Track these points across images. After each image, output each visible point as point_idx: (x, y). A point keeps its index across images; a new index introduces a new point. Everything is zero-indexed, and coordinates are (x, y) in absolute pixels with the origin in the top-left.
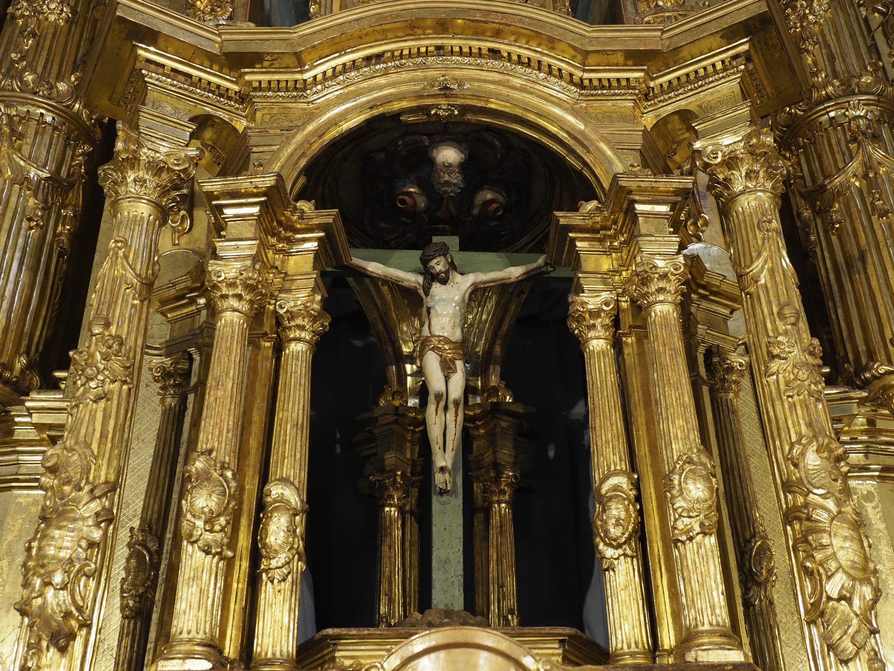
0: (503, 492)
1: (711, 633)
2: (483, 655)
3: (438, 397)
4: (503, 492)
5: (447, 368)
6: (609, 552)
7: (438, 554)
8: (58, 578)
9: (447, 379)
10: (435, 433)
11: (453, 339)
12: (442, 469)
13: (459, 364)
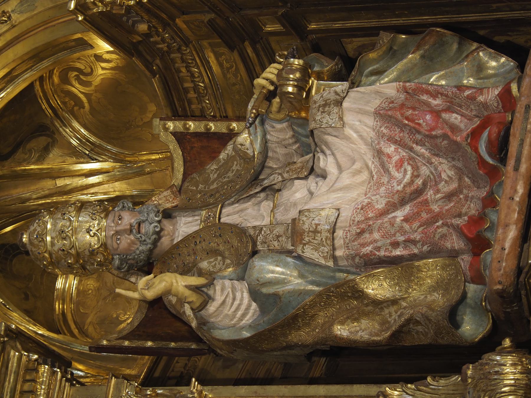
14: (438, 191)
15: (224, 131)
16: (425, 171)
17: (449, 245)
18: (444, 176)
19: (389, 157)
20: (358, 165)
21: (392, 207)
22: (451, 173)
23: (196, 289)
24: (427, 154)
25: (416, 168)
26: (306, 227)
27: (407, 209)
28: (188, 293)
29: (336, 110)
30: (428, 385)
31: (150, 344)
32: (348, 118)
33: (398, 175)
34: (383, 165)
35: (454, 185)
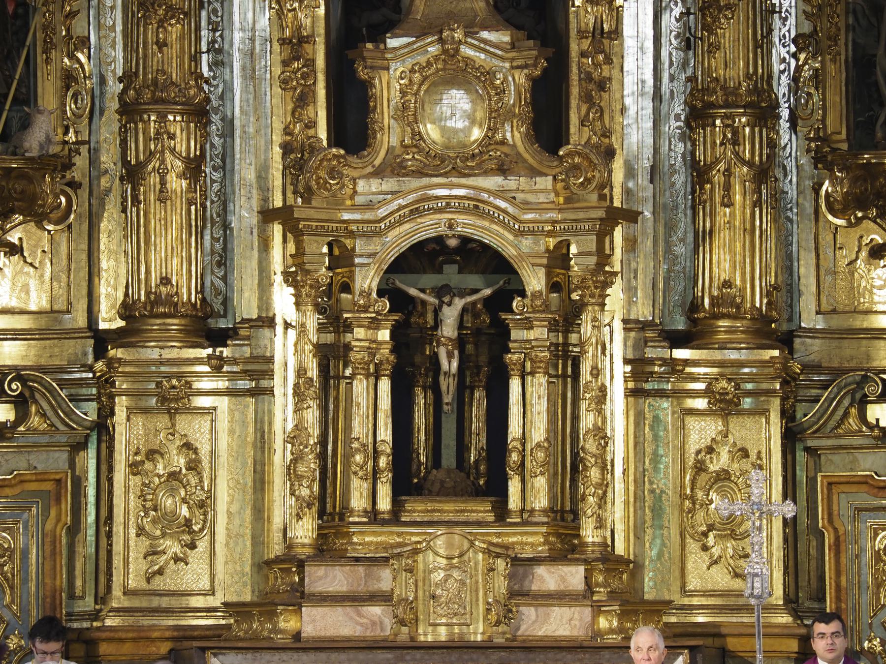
0: (480, 381)
1: (539, 511)
2: (456, 536)
3: (445, 373)
4: (480, 381)
5: (450, 356)
6: (510, 472)
7: (444, 442)
8: (304, 483)
9: (450, 362)
10: (444, 388)
11: (453, 338)
12: (447, 404)
13: (456, 353)
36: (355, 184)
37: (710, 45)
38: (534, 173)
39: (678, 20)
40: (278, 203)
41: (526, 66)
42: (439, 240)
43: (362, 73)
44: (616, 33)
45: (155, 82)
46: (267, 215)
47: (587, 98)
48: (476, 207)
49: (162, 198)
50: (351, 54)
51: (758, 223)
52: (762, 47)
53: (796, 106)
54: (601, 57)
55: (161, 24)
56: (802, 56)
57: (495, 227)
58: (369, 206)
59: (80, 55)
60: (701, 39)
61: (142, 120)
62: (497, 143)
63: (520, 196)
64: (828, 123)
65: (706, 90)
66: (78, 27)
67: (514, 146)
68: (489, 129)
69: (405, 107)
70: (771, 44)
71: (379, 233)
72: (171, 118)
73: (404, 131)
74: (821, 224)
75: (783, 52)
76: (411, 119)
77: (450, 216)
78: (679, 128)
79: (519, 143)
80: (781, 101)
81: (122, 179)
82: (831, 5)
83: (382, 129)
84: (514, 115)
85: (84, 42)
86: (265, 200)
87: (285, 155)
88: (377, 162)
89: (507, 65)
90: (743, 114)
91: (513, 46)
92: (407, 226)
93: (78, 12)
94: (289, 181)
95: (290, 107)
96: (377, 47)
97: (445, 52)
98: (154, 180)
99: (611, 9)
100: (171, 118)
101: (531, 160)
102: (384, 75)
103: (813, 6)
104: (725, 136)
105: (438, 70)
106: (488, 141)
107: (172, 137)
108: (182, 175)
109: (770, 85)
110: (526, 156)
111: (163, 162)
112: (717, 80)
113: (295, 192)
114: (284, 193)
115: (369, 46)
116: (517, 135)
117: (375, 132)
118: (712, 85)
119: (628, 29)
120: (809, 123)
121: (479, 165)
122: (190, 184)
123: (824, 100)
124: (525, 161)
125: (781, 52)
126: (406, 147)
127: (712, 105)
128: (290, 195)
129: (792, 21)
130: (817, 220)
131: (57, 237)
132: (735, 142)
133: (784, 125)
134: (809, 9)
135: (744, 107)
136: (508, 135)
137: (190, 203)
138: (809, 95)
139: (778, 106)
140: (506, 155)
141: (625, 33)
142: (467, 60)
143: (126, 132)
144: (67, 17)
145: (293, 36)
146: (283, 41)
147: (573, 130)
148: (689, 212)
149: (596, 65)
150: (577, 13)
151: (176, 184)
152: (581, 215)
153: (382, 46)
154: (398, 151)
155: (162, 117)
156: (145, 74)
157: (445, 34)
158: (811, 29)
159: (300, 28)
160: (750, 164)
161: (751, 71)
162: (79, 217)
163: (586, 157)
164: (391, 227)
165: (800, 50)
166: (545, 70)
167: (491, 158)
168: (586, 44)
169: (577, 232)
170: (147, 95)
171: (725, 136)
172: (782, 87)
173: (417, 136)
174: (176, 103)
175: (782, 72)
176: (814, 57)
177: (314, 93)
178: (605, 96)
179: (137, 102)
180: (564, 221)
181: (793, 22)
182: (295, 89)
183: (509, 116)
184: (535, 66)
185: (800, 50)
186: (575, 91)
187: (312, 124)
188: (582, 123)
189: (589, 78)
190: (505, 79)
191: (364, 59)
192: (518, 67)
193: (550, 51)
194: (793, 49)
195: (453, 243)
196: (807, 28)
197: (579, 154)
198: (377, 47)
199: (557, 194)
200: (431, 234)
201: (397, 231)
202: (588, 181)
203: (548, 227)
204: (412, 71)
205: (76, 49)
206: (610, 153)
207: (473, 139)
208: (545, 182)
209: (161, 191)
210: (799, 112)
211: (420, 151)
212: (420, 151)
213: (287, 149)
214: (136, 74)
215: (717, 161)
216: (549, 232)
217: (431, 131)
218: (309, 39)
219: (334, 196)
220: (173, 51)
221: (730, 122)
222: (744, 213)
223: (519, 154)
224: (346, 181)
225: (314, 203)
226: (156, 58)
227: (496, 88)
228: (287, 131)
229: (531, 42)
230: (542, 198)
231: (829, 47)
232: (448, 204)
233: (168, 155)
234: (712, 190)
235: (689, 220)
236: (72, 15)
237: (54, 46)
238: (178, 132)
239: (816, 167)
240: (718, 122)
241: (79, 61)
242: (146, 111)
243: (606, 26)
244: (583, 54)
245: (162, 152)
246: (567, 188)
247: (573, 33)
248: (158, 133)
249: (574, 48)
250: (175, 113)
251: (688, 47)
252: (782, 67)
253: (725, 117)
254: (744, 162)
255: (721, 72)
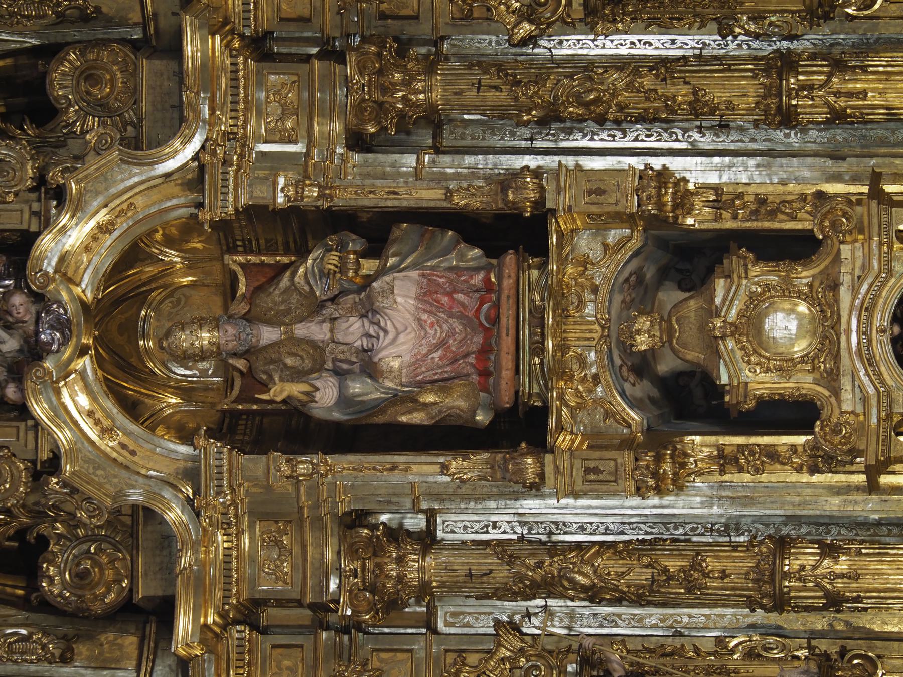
14: (455, 340)
15: (273, 262)
16: (445, 327)
17: (465, 372)
18: (457, 330)
19: (425, 322)
20: (409, 330)
21: (430, 352)
22: (460, 327)
23: (306, 393)
24: (446, 317)
25: (441, 327)
26: (384, 368)
27: (440, 352)
28: (300, 395)
29: (391, 296)
30: (470, 459)
31: (255, 407)
32: (399, 300)
33: (432, 332)
34: (421, 326)
35: (463, 335)
36: (846, 412)
37: (727, 109)
38: (837, 259)
39: (704, 136)
40: (861, 479)
41: (746, 266)
42: (894, 341)
43: (751, 405)
44: (717, 189)
45: (755, 581)
46: (872, 487)
47: (772, 214)
48: (867, 310)
49: (854, 576)
50: (734, 414)
51: (881, 69)
52: (730, 65)
53: (780, 35)
54: (738, 202)
55: (706, 575)
56: (737, 30)
57: (884, 294)
58: (865, 400)
59: (732, 645)
60: (722, 116)
61: (788, 593)
62: (811, 291)
63: (857, 272)
64: (795, 8)
65: (766, 113)
66: (708, 646)
67: (813, 276)
68: (799, 298)
69: (780, 369)
70: (725, 57)
71: (889, 394)
72: (786, 568)
73: (800, 371)
74: (881, 14)
75: (733, 46)
76: (790, 364)
77: (874, 332)
78: (796, 135)
79: (811, 272)
80: (775, 47)
81: (838, 611)
82: (694, 6)
83: (798, 389)
84: (787, 276)
85: (719, 641)
86: (858, 489)
87: (820, 472)
88: (827, 393)
89: (744, 282)
90: (787, 81)
91: (728, 277)
92: (883, 369)
93: (694, 645)
94: (842, 469)
95: (778, 467)
96: (729, 392)
97: (733, 335)
98: (839, 584)
99: (697, 193)
100: (786, 568)
101: (826, 263)
102: (751, 386)
103: (695, 21)
104: (805, 97)
105: (748, 341)
106: (809, 298)
107: (802, 567)
108: (836, 560)
109: (762, 58)
110: (822, 266)
111: (824, 576)
112: (757, 103)
113: (852, 463)
114: (853, 473)
115: (727, 398)
116: (804, 274)
117: (801, 395)
118: (762, 107)
119: (713, 178)
120: (794, 24)
121: (830, 306)
122: (844, 553)
123: (775, 12)
124: (827, 267)
125: (731, 47)
126: (813, 369)
127: (779, 108)
128: (854, 468)
129: (706, 39)
130: (878, 18)
131: (888, 668)
132: (811, 88)
133: (794, 45)
134: (697, 25)
135: (781, 81)
136: (805, 281)
137: (859, 553)
138: (770, 24)
139: (778, 51)
140: (822, 283)
141: (717, 181)
142: (740, 315)
143: (798, 607)
144: (698, 655)
145: (718, 463)
146: (722, 472)
147: (798, 226)
148: (869, 127)
149: (744, 206)
150: (700, 222)
151: (843, 565)
152: (875, 220)
153: (728, 388)
154: (818, 376)
155: (786, 576)
156: (749, 589)
157: (718, 334)
158: (714, 22)
159: (711, 457)
160: (830, 75)
161: (750, 74)
162: (870, 649)
163: (825, 216)
164: (883, 382)
165: (732, 32)
166: (749, 250)
167: (824, 296)
168: (726, 215)
169: (889, 224)
170: (767, 588)
171: (805, 97)
172: (764, 48)
173: (803, 359)
174: (774, 563)
175: (749, 46)
176: (737, 20)
177: (766, 446)
178: (770, 199)
179: (773, 597)
180: (879, 235)
181: (707, 37)
182: (763, 462)
183: (787, 280)
184: (745, 258)
185: (732, 32)
186: (766, 224)
187: (793, 448)
188: (794, 218)
189: (755, 212)
190: (756, 284)
191: (738, 403)
192: (746, 273)
193: (733, 245)
194: (730, 38)
195: (897, 330)
196: (714, 26)
197: (822, 221)
198: (729, 392)
199: (856, 240)
200: (889, 348)
201: (887, 377)
202: (845, 214)
203: (885, 249)
204: (749, 362)
205: (726, 648)
206: (820, 195)
207: (807, 312)
208: (846, 250)
209: (850, 578)
210: (786, 32)
211: (817, 356)
212: (817, 356)
213: (814, 470)
214: (749, 597)
215: (827, 104)
216: (889, 248)
217: (800, 347)
218: (721, 449)
219: (855, 430)
220: (730, 566)
221: (794, 93)
222: (873, 81)
223: (821, 273)
224: (842, 420)
225: (862, 447)
226: (735, 580)
227: (764, 292)
228: (799, 469)
229: (725, 261)
230: (859, 253)
231: (730, 7)
232: (864, 334)
233: (818, 572)
234: (852, 107)
235: (875, 126)
236: (697, 651)
237: (723, 666)
238: (798, 562)
239: (833, 18)
240: (794, 102)
241: (737, 646)
242: (781, 589)
243: (712, 198)
244: (735, 217)
245: (816, 576)
246: (850, 232)
247: (717, 226)
248: (799, 580)
249: (730, 225)
250: (783, 565)
251: (727, 126)
252: (745, 47)
253: (789, 97)
254: (828, 81)
255: (751, 99)
